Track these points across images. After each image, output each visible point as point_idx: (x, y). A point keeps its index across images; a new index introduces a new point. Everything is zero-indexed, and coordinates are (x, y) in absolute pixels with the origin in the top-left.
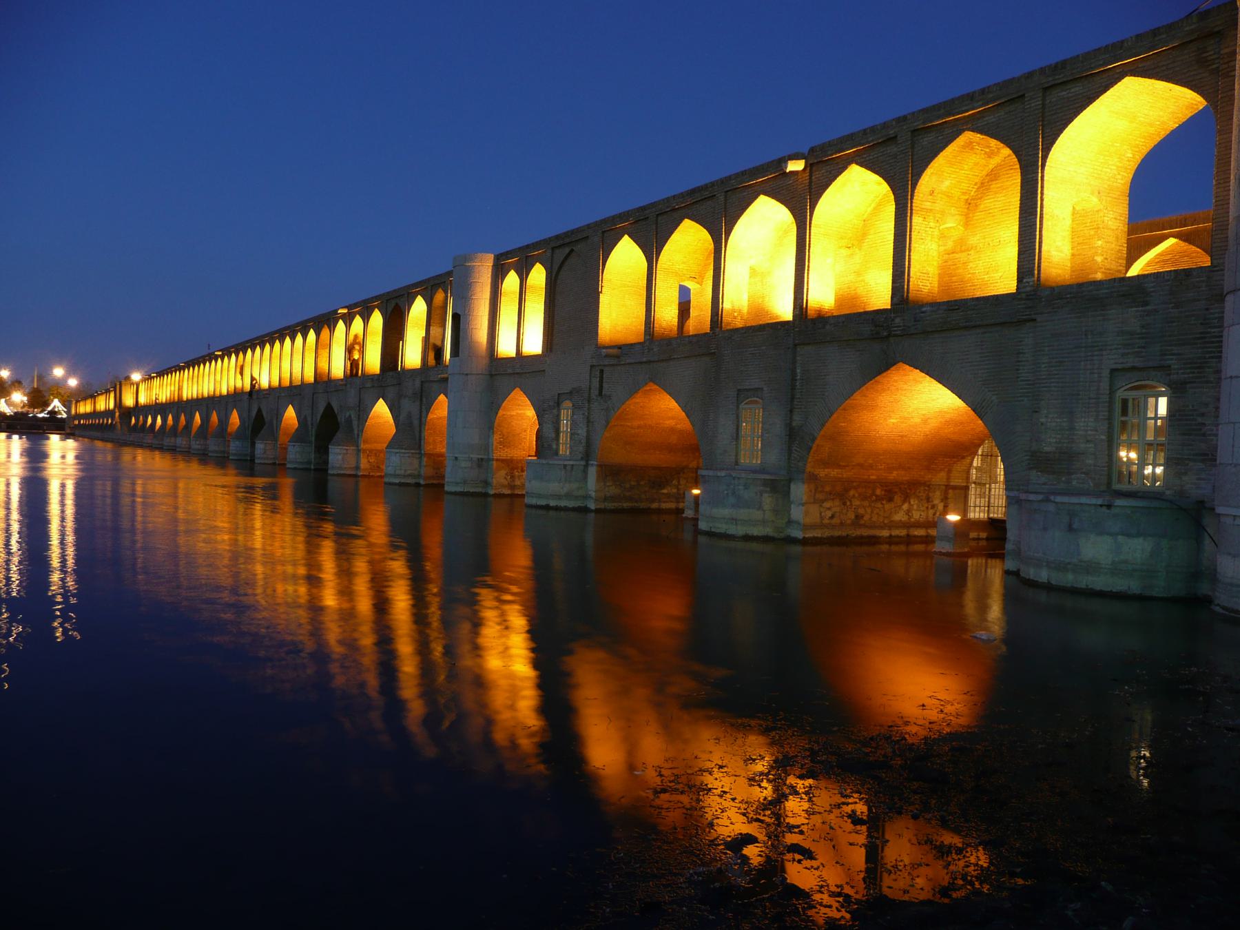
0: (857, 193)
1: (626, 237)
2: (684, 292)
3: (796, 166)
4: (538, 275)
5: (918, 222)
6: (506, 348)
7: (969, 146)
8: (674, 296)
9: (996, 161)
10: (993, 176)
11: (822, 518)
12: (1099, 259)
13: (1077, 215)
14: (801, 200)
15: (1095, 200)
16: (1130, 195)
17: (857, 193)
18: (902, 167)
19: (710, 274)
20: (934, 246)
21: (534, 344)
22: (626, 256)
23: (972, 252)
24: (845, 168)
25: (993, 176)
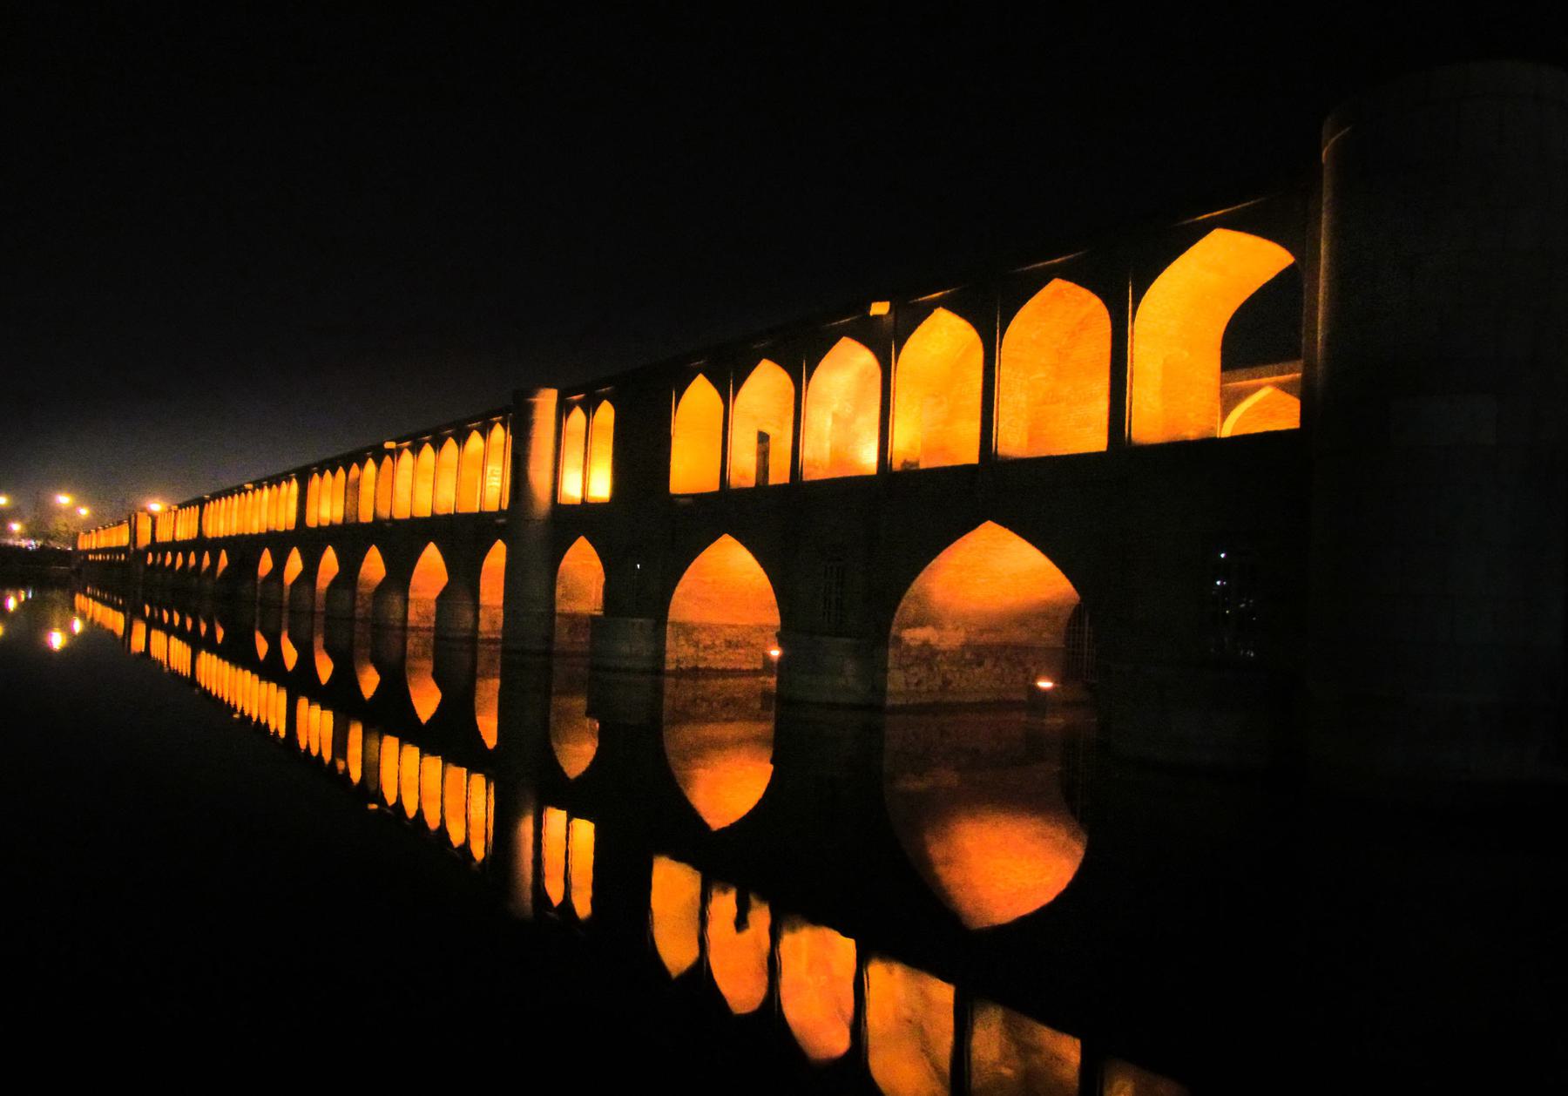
0: (943, 337)
1: (701, 377)
2: (763, 438)
3: (880, 309)
4: (606, 414)
5: (1004, 372)
6: (571, 490)
7: (1058, 294)
8: (753, 439)
9: (1085, 310)
10: (1083, 325)
11: (907, 684)
12: (1191, 415)
13: (1168, 370)
14: (886, 344)
15: (1186, 354)
16: (1224, 348)
17: (943, 337)
18: (990, 316)
19: (790, 418)
20: (1024, 398)
21: (601, 487)
22: (700, 395)
23: (1063, 405)
24: (931, 312)
25: (1083, 325)
